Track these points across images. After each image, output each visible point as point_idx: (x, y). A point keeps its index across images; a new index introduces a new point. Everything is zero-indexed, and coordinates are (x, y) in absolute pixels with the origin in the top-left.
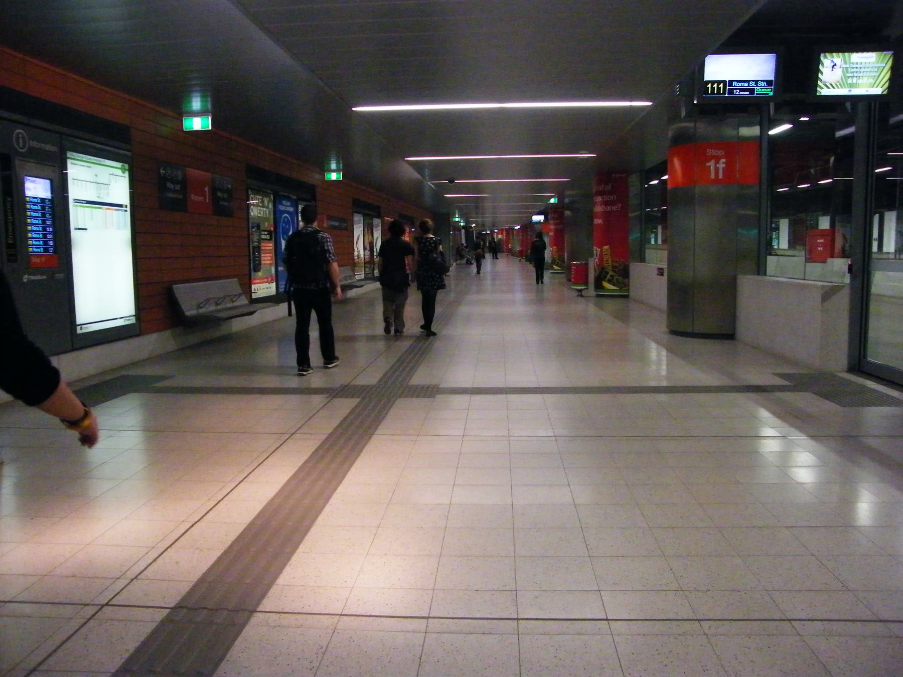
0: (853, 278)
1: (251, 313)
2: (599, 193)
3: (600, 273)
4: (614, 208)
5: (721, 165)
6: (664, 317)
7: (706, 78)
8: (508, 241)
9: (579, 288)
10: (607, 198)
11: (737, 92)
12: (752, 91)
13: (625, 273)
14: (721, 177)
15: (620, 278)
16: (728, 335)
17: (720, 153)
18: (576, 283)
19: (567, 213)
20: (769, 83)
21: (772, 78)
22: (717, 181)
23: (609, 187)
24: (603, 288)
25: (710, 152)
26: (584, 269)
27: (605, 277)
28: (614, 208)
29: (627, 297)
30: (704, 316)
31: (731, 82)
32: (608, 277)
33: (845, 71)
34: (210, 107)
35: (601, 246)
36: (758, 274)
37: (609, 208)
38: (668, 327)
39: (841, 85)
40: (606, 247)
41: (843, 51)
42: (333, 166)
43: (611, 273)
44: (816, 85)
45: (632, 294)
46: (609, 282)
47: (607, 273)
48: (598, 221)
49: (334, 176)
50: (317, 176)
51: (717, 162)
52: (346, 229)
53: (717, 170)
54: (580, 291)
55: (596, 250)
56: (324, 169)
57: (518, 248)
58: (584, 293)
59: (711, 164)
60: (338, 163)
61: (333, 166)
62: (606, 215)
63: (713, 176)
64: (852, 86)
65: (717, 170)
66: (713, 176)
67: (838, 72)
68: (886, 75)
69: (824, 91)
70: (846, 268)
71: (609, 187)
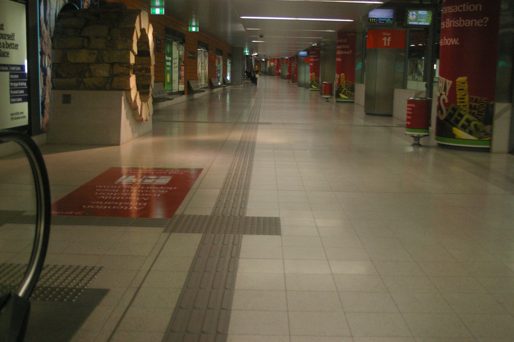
0: (427, 89)
1: (172, 99)
2: (339, 44)
3: (339, 89)
4: (348, 53)
5: (389, 40)
6: (363, 109)
7: (370, 16)
8: (278, 67)
9: (327, 97)
10: (344, 47)
11: (380, 22)
12: (385, 22)
13: (352, 89)
14: (388, 45)
15: (349, 92)
16: (391, 116)
17: (389, 34)
18: (325, 94)
19: (322, 52)
20: (391, 19)
21: (392, 18)
22: (386, 47)
23: (345, 41)
24: (339, 97)
25: (384, 34)
26: (331, 86)
27: (341, 91)
28: (348, 53)
29: (353, 102)
30: (379, 108)
31: (378, 19)
32: (343, 91)
33: (417, 16)
34: (164, 3)
35: (339, 74)
36: (403, 88)
37: (345, 53)
38: (365, 112)
39: (416, 20)
40: (342, 74)
41: (416, 10)
42: (194, 24)
43: (345, 89)
44: (407, 21)
45: (355, 101)
46: (344, 93)
47: (342, 89)
48: (339, 60)
49: (194, 29)
50: (186, 29)
51: (387, 39)
52: (195, 58)
53: (387, 41)
54: (327, 98)
55: (337, 76)
56: (188, 25)
57: (287, 73)
58: (329, 100)
59: (385, 39)
60: (196, 22)
61: (194, 24)
62: (343, 56)
63: (385, 45)
64: (419, 21)
65: (387, 41)
66: (385, 45)
67: (415, 17)
68: (430, 19)
69: (410, 23)
70: (424, 85)
71: (345, 41)
